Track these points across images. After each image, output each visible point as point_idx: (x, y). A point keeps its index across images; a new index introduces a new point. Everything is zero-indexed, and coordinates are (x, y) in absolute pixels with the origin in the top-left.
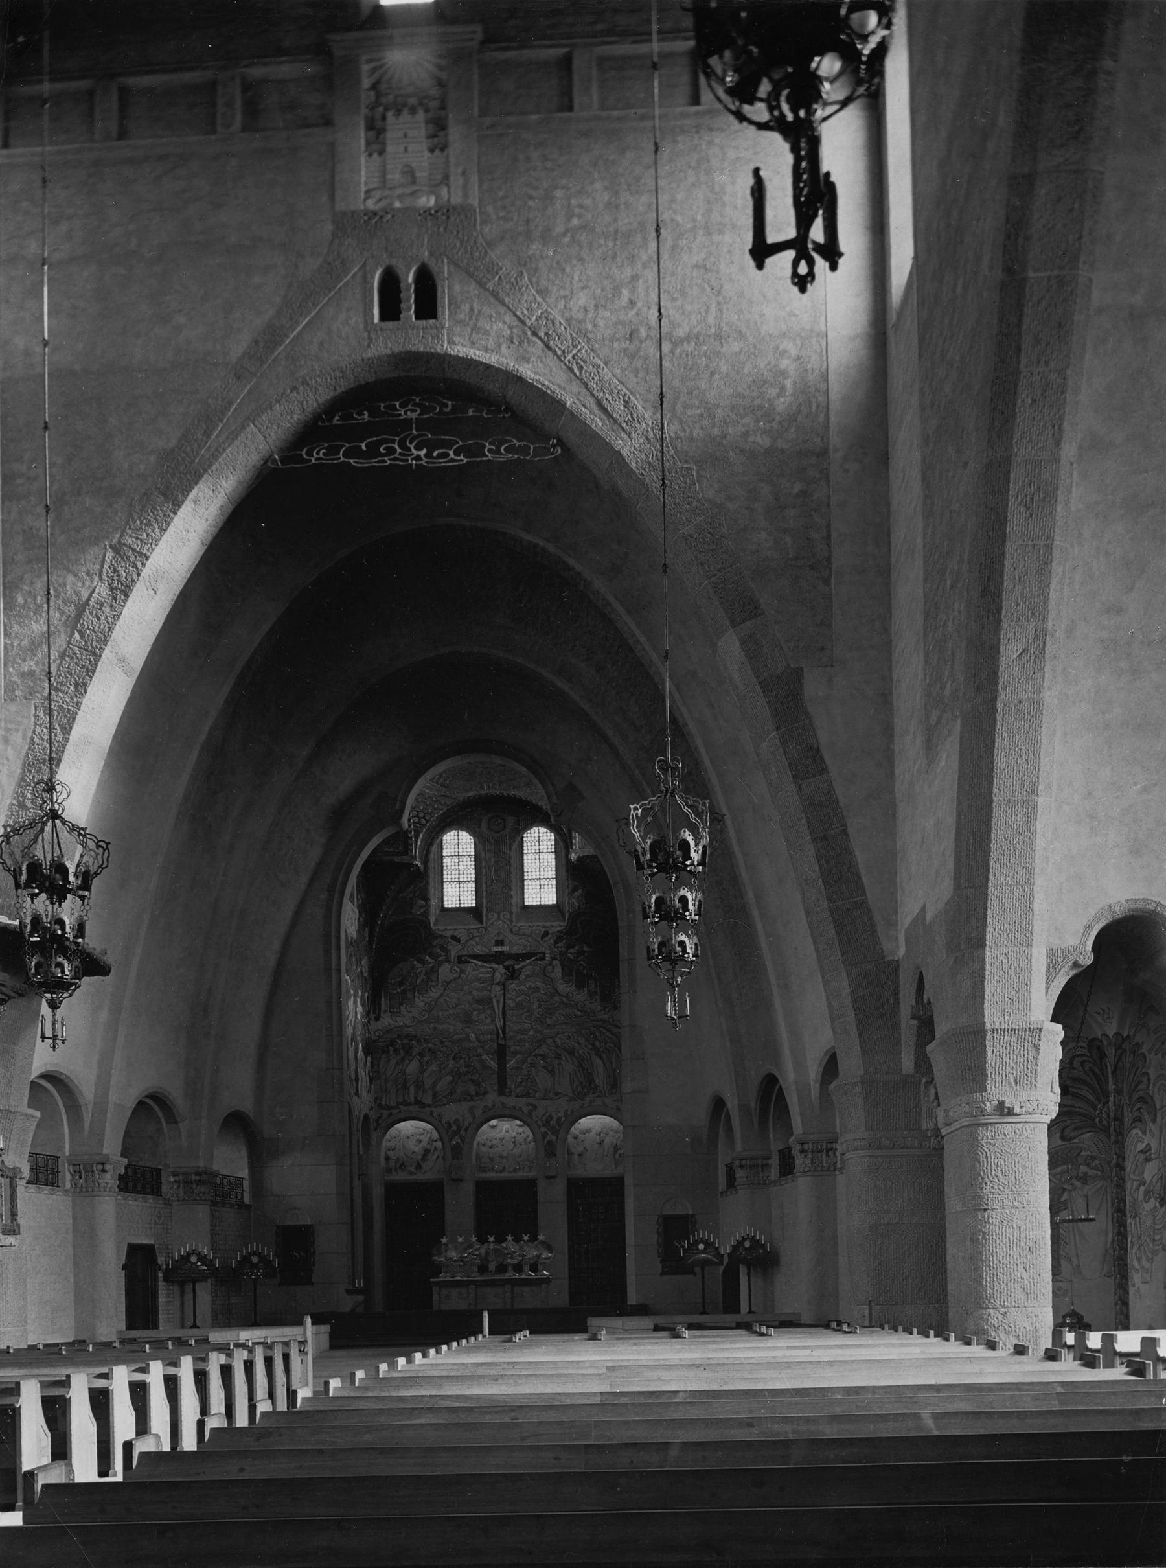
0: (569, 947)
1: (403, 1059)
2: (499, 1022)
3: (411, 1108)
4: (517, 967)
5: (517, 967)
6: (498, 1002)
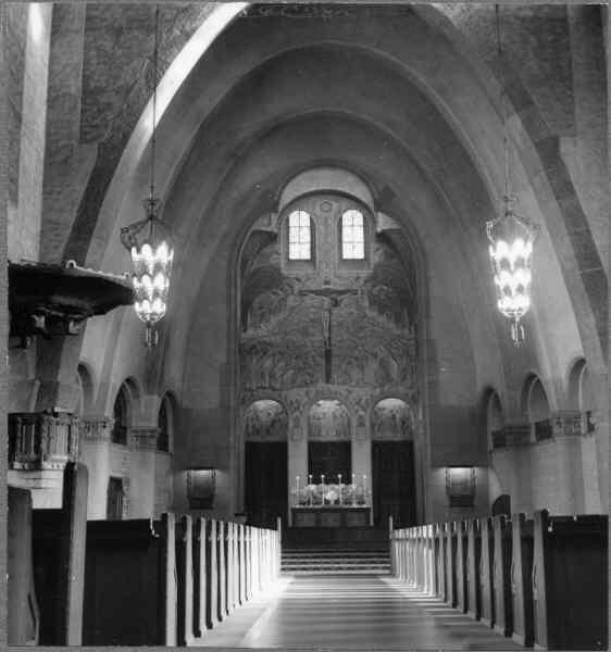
2: (327, 335)
5: (339, 298)
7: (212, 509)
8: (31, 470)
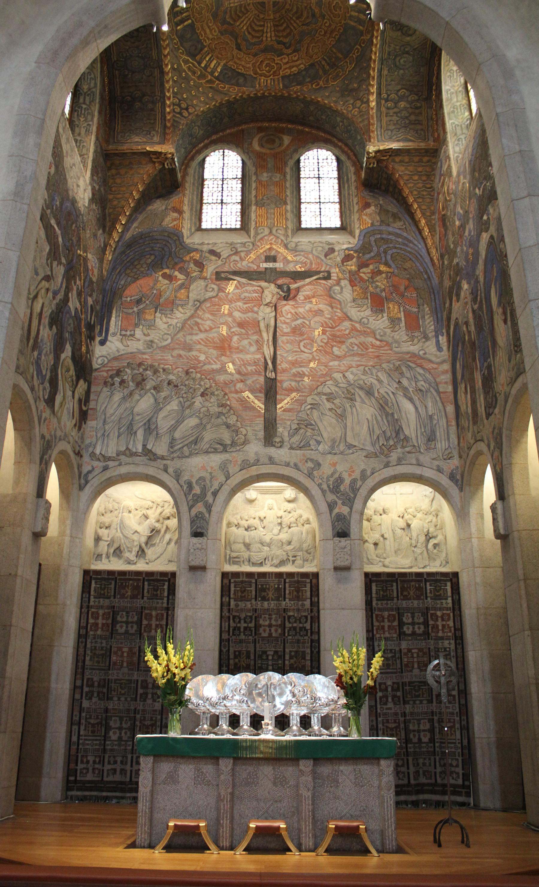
0: (362, 265)
1: (131, 394)
2: (268, 351)
3: (137, 459)
5: (293, 286)
6: (267, 326)
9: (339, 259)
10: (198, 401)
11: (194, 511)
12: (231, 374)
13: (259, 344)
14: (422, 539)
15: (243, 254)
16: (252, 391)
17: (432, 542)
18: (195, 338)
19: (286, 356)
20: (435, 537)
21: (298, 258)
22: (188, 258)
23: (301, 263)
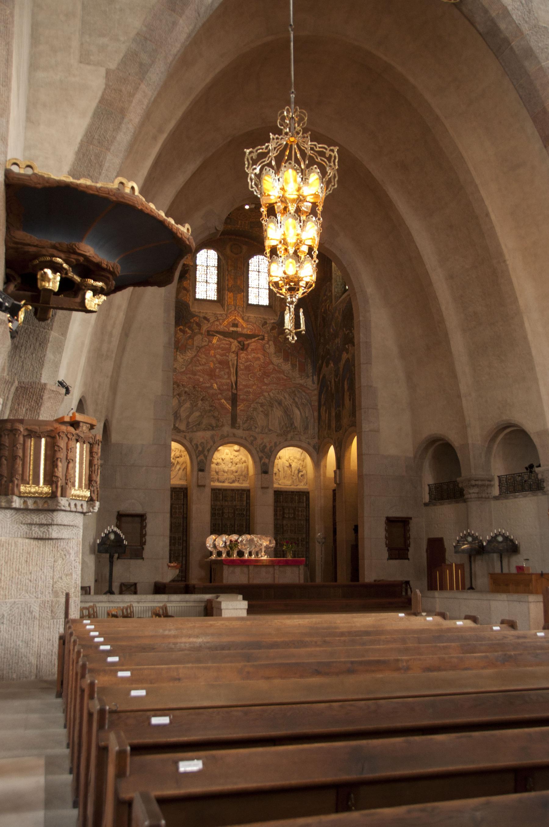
2: (233, 379)
4: (246, 343)
5: (246, 343)
6: (233, 365)
7: (143, 559)
8: (37, 511)
9: (269, 329)
10: (200, 403)
11: (199, 459)
12: (215, 390)
13: (229, 374)
14: (296, 472)
15: (221, 321)
16: (226, 399)
17: (301, 474)
18: (197, 368)
19: (242, 382)
20: (302, 471)
21: (249, 326)
22: (192, 321)
23: (250, 329)
